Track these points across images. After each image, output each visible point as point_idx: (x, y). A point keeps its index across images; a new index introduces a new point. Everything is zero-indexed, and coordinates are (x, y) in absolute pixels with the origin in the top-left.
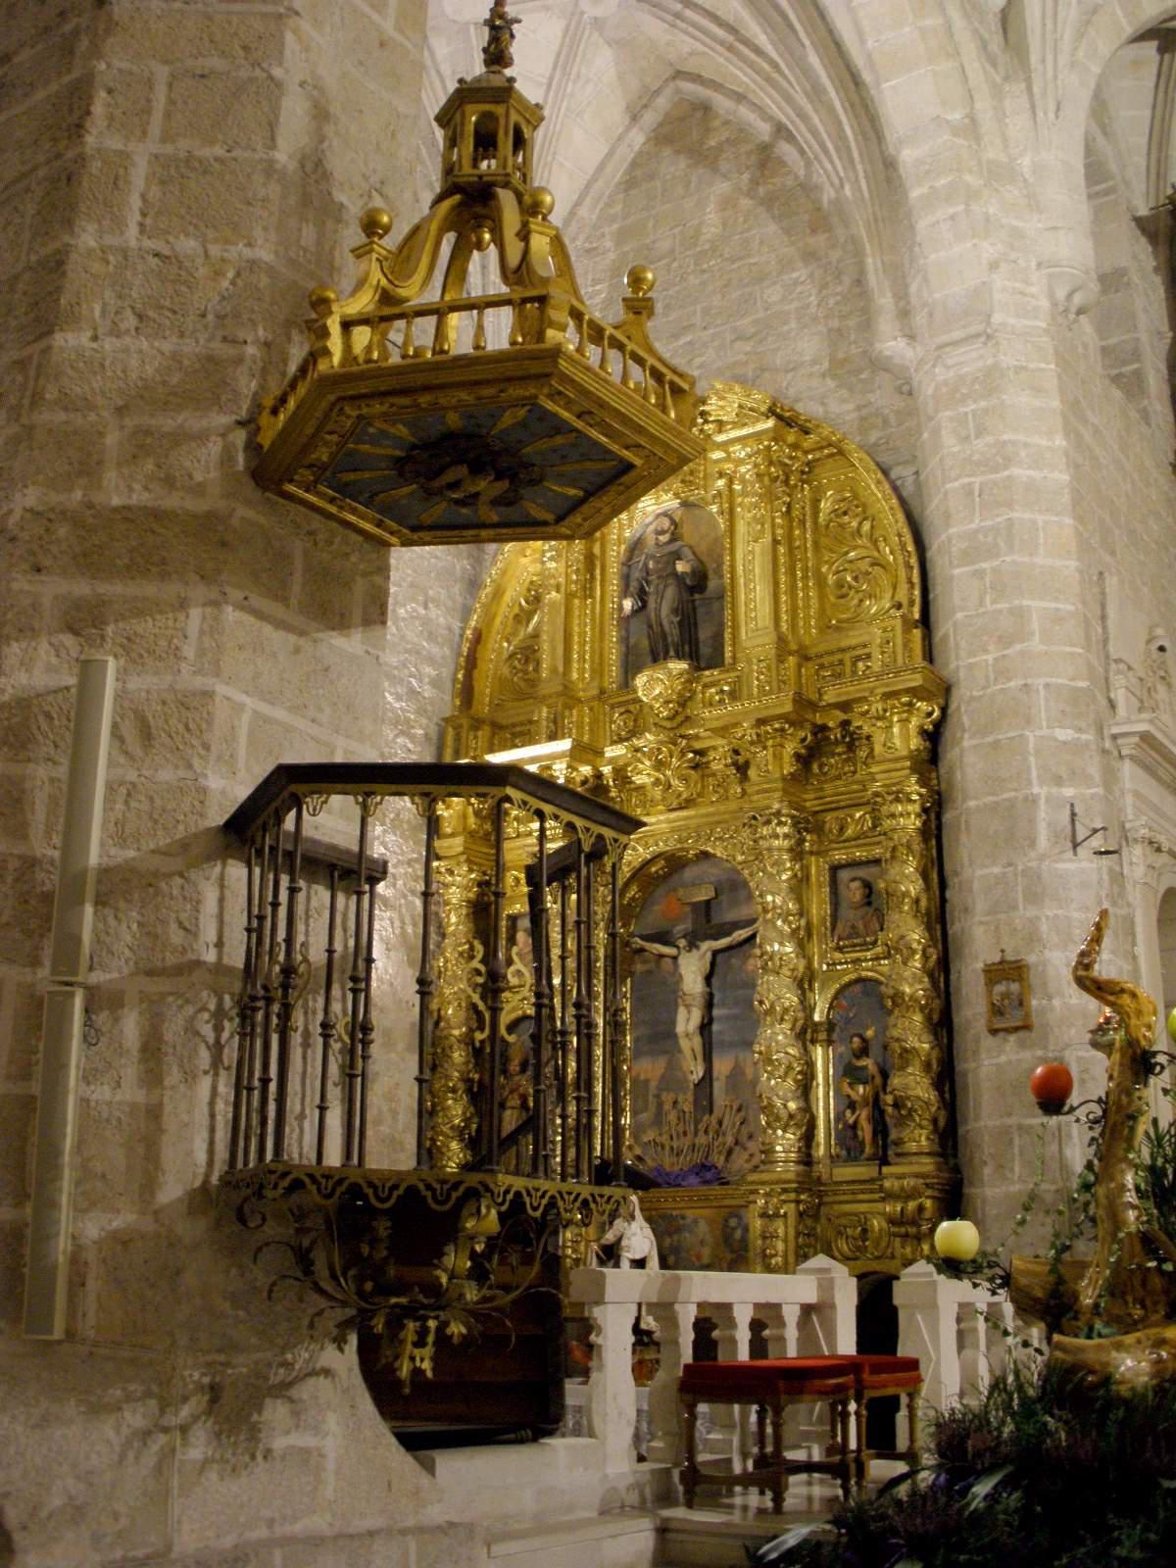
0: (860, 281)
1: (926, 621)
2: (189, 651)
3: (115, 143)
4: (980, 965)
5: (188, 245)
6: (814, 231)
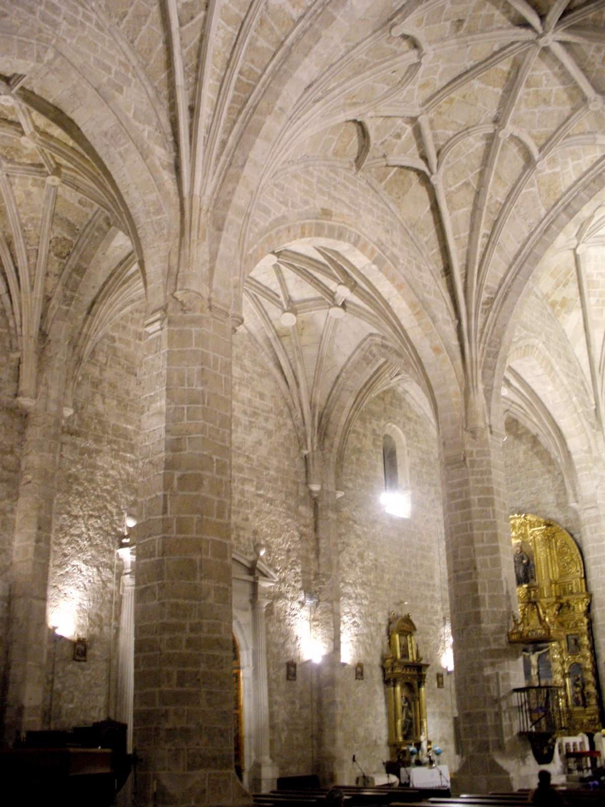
0: (563, 481)
1: (585, 577)
3: (483, 594)
5: (495, 609)
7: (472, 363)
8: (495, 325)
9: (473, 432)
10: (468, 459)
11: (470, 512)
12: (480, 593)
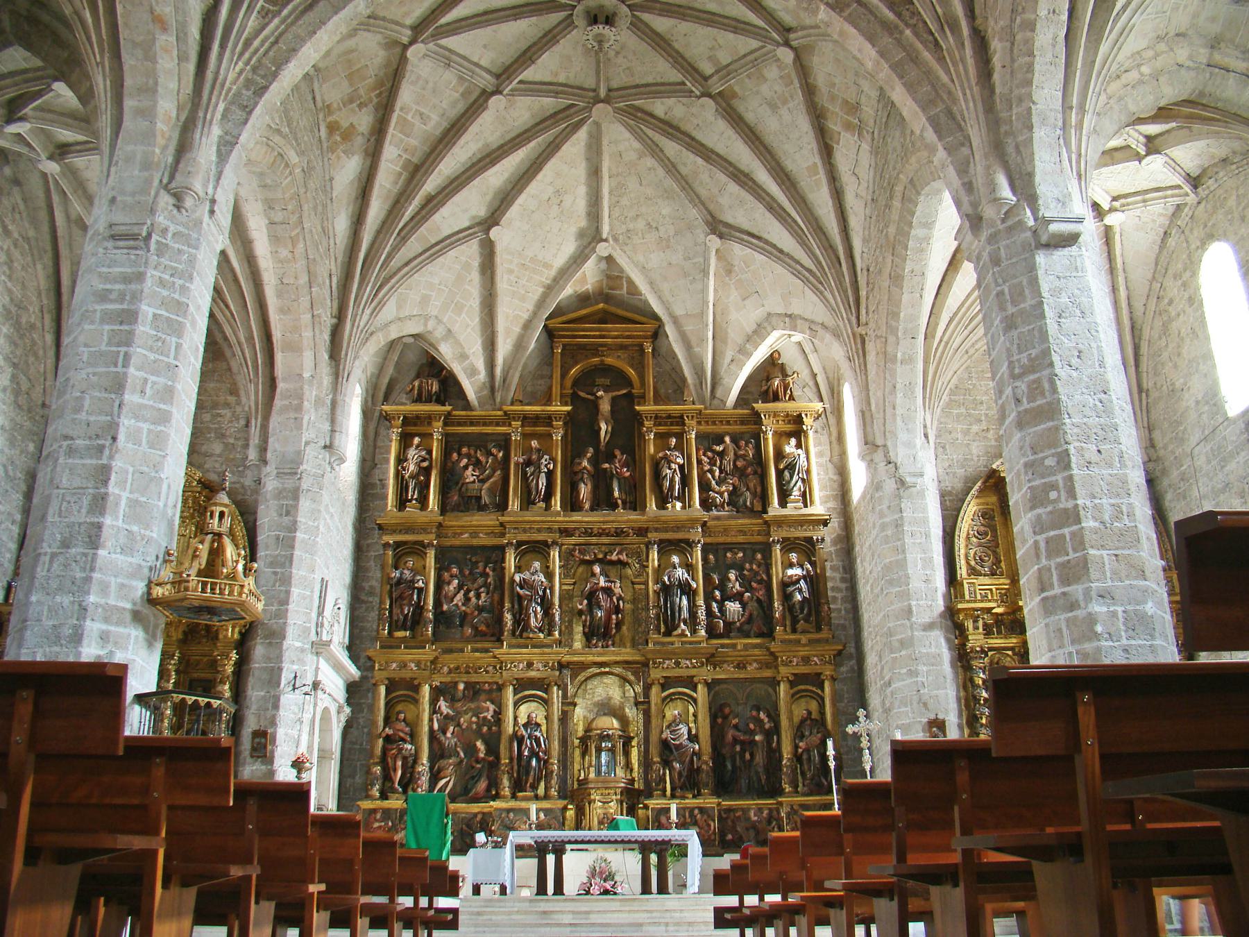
2: (130, 648)
3: (117, 491)
4: (250, 730)
5: (135, 528)
6: (231, 394)
7: (215, 80)
8: (276, 42)
9: (178, 198)
10: (155, 237)
11: (131, 333)
12: (112, 488)
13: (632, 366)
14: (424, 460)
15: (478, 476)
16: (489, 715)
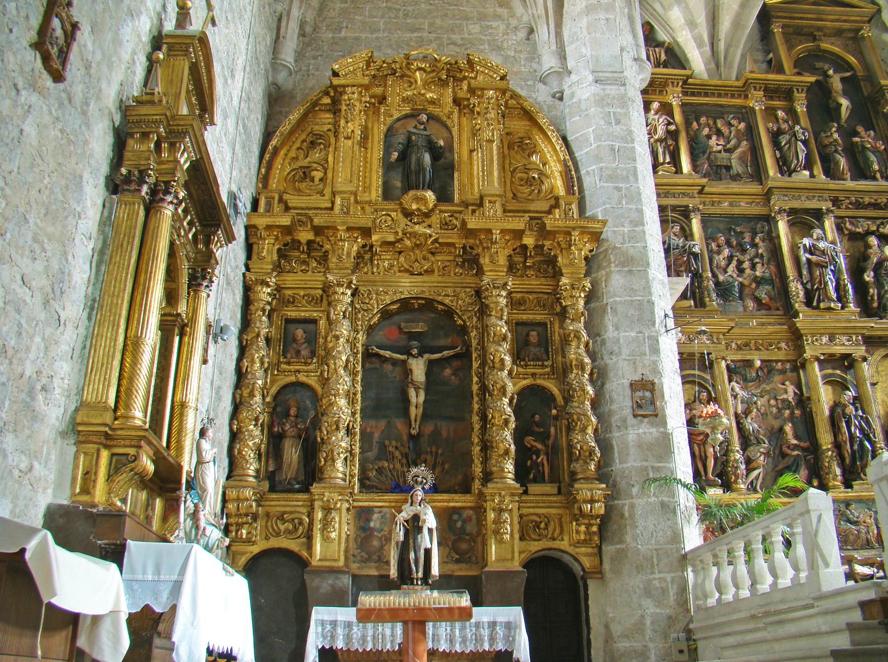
4: (626, 382)
6: (501, 6)
13: (848, 52)
14: (669, 124)
15: (724, 146)
16: (790, 396)
